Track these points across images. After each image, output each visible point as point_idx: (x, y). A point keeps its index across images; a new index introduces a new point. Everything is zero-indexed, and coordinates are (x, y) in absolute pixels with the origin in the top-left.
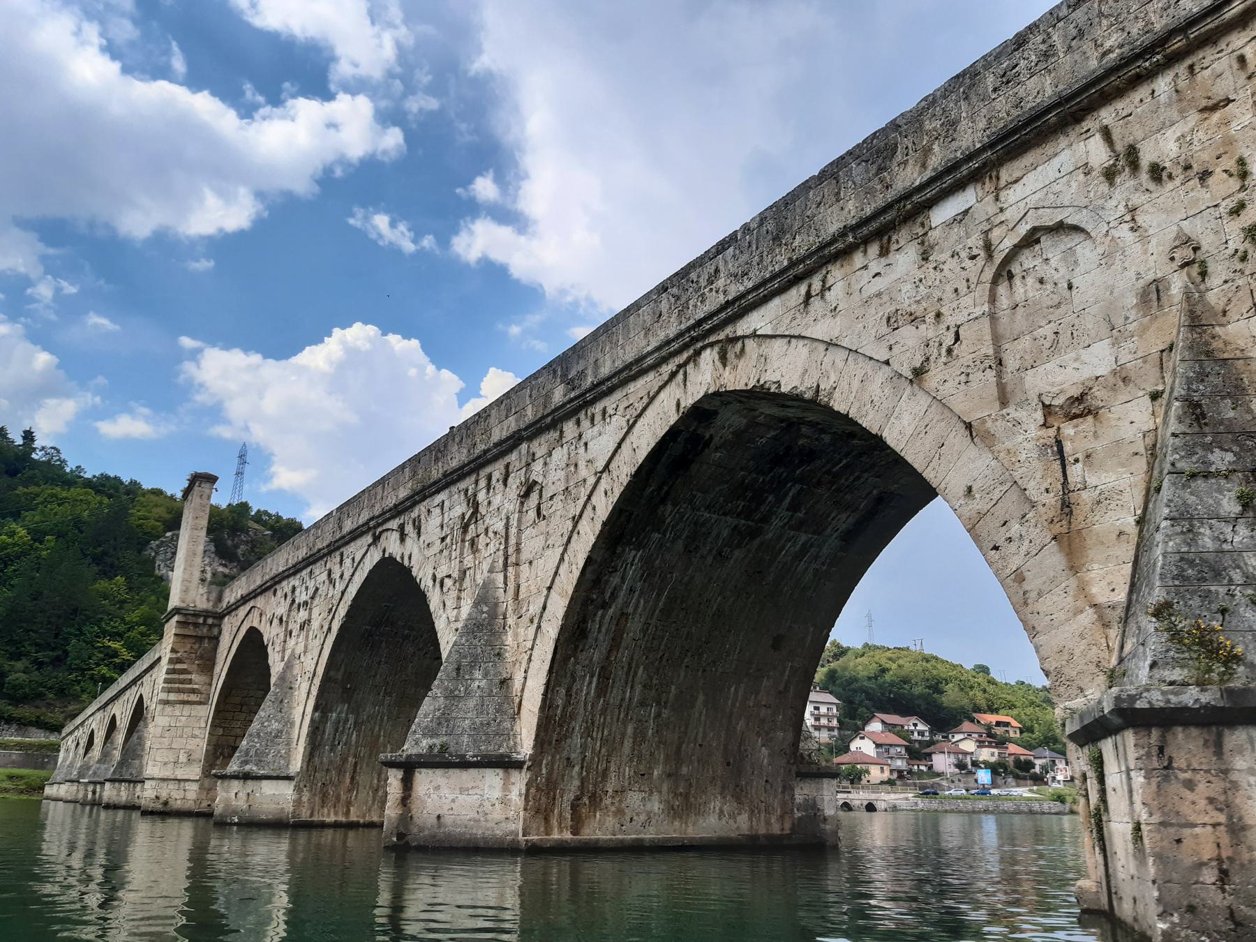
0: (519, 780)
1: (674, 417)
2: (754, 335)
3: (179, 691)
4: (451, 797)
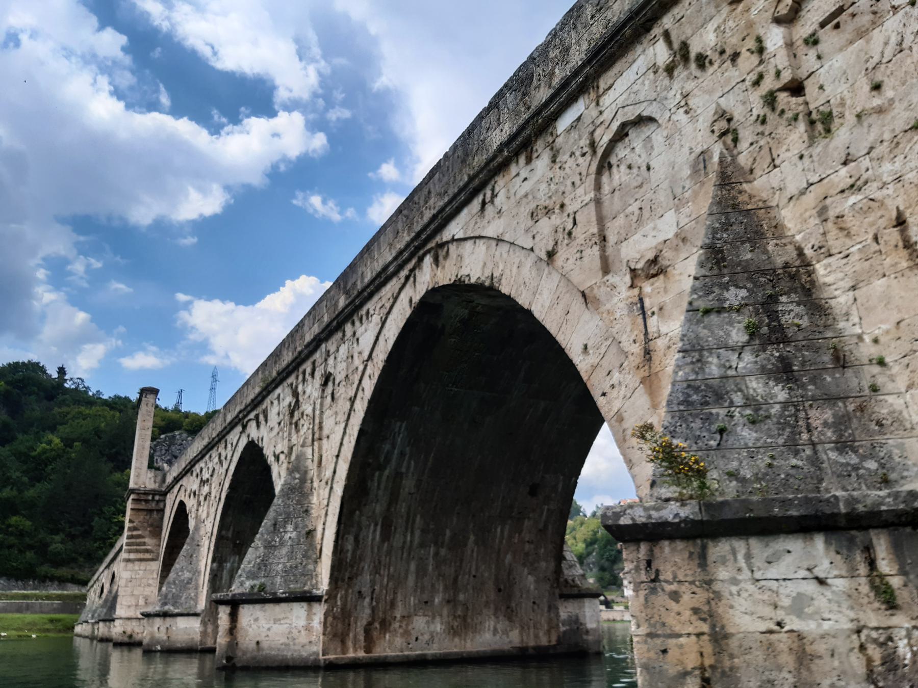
0: (319, 610)
1: (408, 312)
2: (453, 240)
3: (137, 551)
4: (267, 626)
